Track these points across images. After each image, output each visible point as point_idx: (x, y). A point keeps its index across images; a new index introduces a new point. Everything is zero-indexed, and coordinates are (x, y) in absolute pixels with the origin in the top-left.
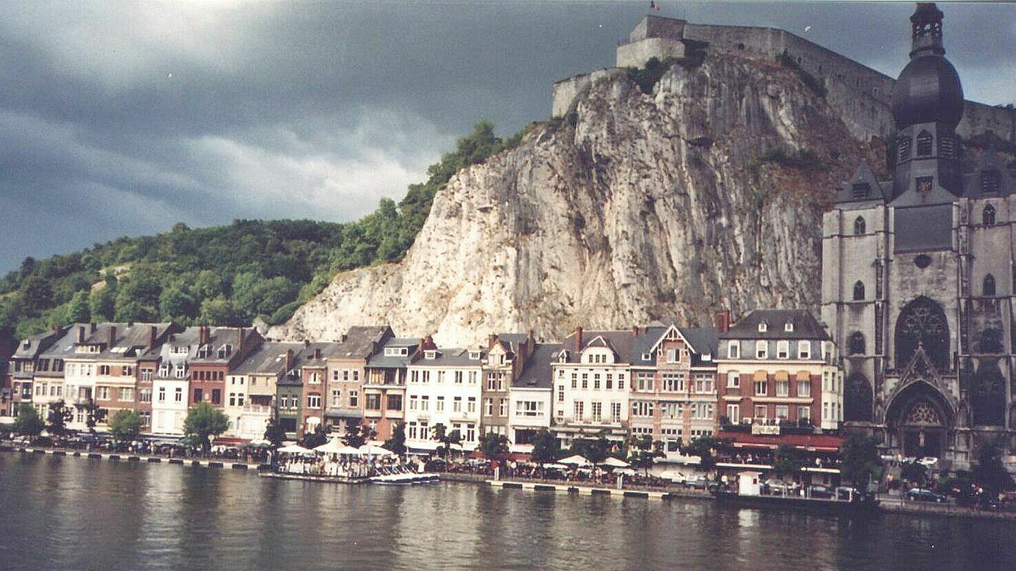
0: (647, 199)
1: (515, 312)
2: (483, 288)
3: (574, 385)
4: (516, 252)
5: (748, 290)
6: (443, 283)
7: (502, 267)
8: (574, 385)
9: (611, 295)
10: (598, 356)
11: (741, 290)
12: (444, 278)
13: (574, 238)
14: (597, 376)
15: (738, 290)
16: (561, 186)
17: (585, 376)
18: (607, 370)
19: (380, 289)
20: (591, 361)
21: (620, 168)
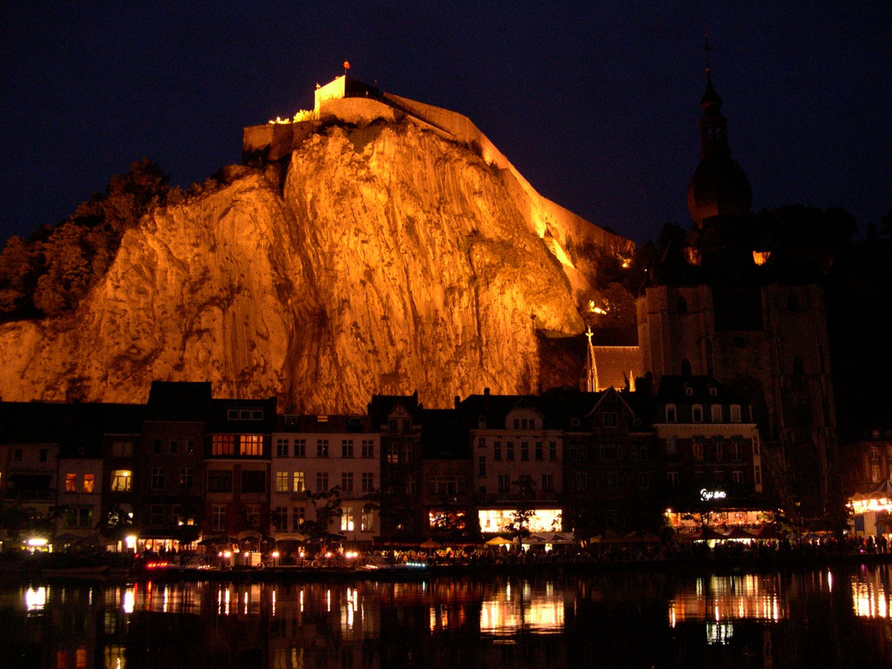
0: (364, 268)
1: (224, 386)
2: (187, 355)
3: (498, 454)
4: (221, 312)
5: (471, 374)
6: (133, 347)
7: (207, 330)
8: (498, 454)
9: (334, 373)
10: (524, 422)
11: (463, 374)
12: (134, 339)
13: (280, 304)
14: (525, 445)
15: (460, 374)
16: (263, 243)
17: (510, 445)
18: (536, 437)
19: (47, 349)
20: (516, 426)
21: (338, 228)
